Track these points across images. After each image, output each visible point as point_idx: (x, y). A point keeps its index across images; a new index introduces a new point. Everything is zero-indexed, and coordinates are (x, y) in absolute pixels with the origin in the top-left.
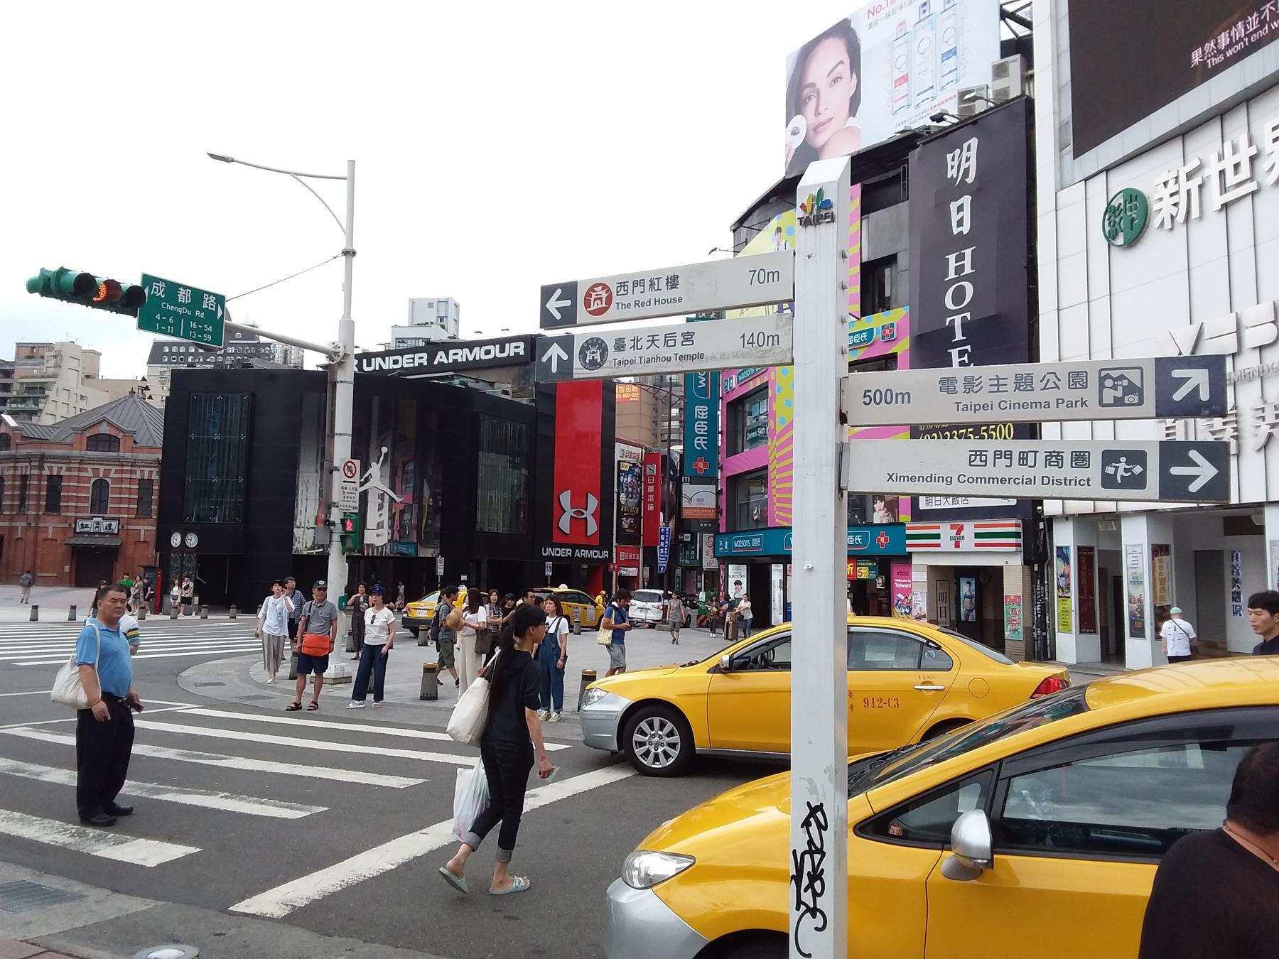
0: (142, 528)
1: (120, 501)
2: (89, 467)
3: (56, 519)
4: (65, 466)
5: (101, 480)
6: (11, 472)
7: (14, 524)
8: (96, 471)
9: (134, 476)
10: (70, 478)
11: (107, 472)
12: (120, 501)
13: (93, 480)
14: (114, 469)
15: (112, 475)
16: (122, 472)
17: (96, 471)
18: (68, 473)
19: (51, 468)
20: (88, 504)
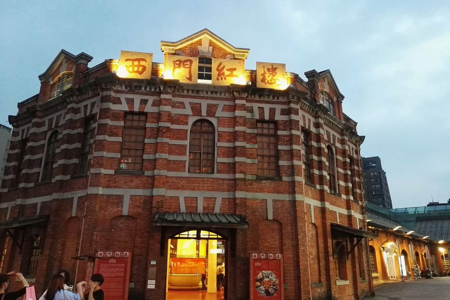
0: (270, 197)
1: (233, 152)
2: (187, 101)
3: (137, 181)
4: (151, 99)
5: (202, 121)
6: (68, 117)
7: (68, 195)
8: (196, 110)
9: (248, 115)
10: (158, 117)
11: (211, 111)
12: (233, 152)
13: (192, 120)
14: (221, 104)
15: (219, 113)
16: (234, 108)
17: (196, 110)
18: (155, 110)
19: (130, 102)
20: (186, 158)
